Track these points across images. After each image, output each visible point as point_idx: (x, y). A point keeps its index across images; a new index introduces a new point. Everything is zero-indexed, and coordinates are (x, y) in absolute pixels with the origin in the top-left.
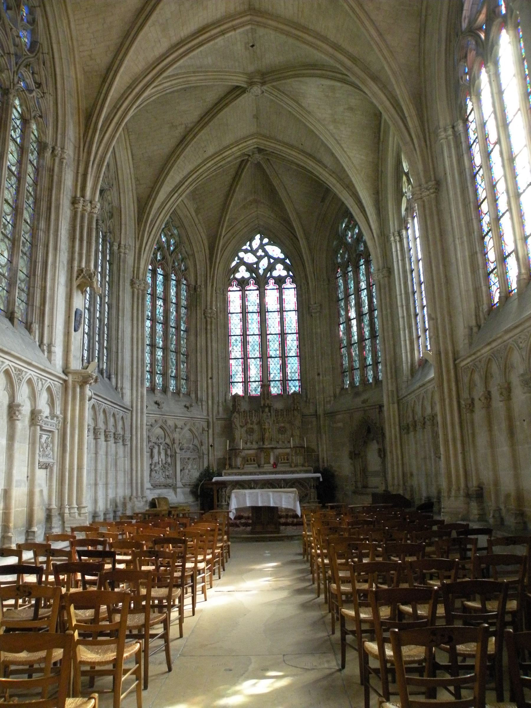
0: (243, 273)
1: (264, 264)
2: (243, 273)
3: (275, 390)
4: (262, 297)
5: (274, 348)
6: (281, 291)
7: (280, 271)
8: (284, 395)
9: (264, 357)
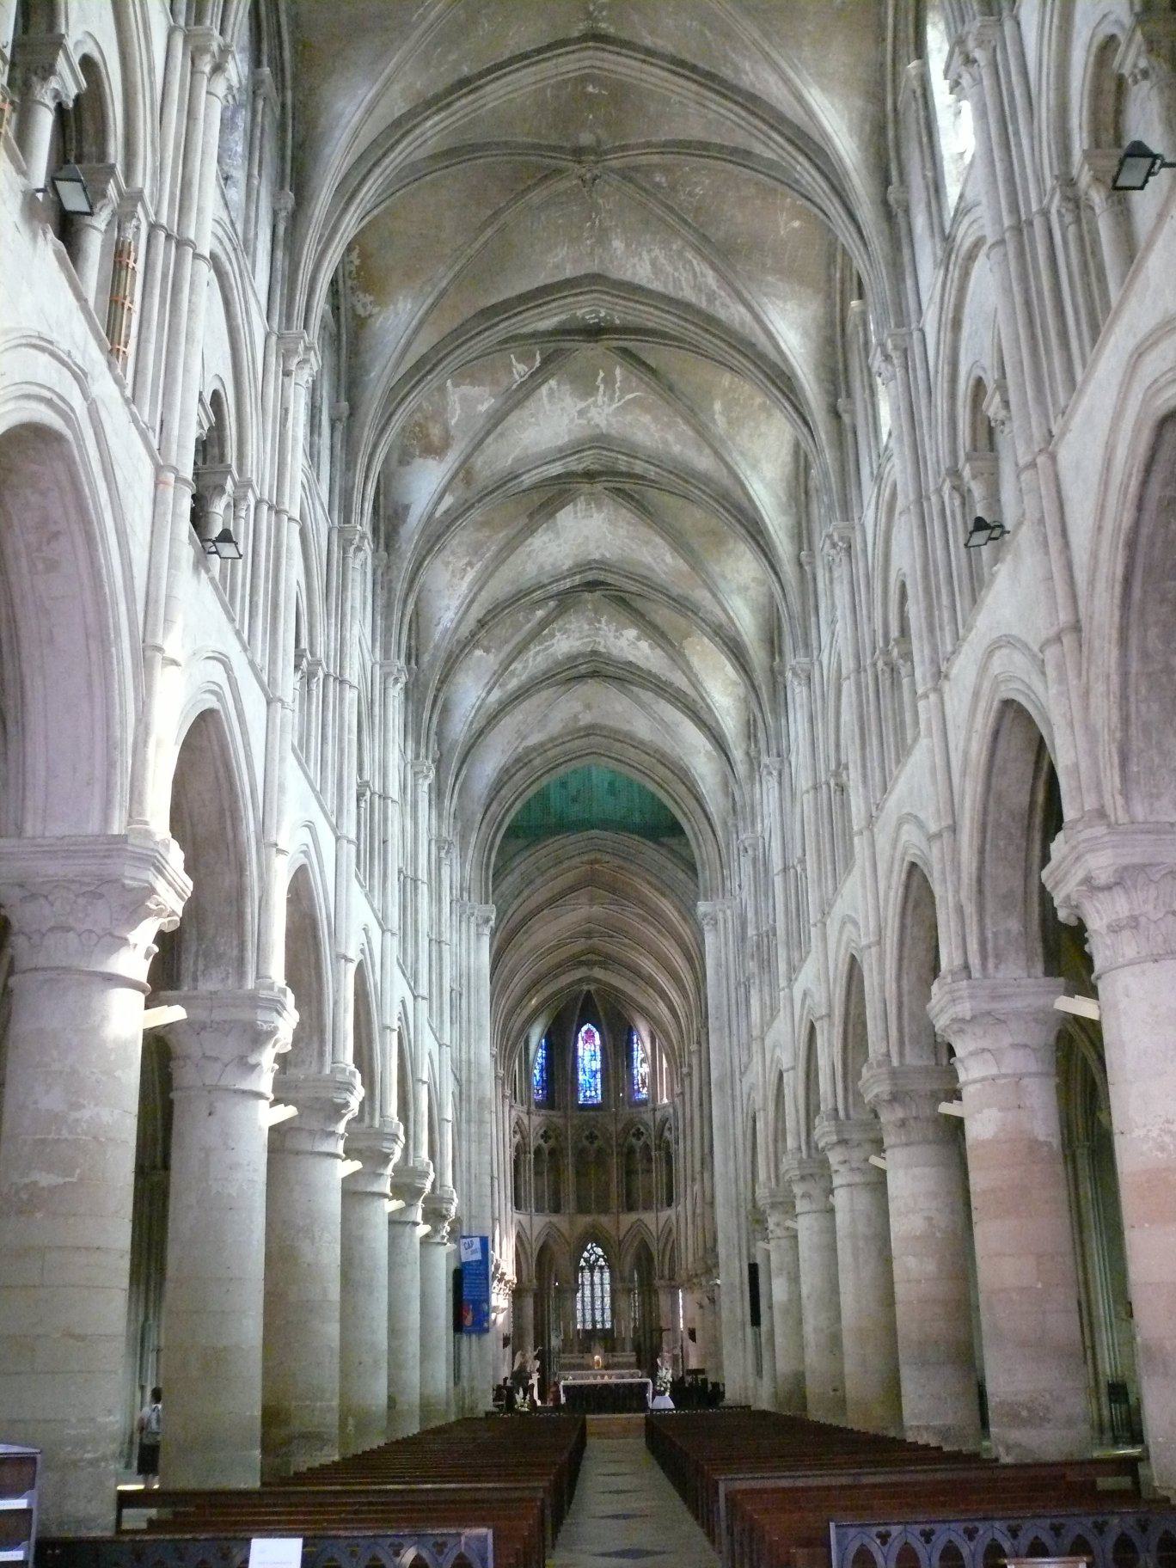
0: (582, 1263)
1: (593, 1258)
2: (582, 1263)
3: (599, 1326)
4: (592, 1276)
5: (598, 1303)
6: (602, 1274)
7: (601, 1262)
8: (603, 1330)
9: (593, 1309)
